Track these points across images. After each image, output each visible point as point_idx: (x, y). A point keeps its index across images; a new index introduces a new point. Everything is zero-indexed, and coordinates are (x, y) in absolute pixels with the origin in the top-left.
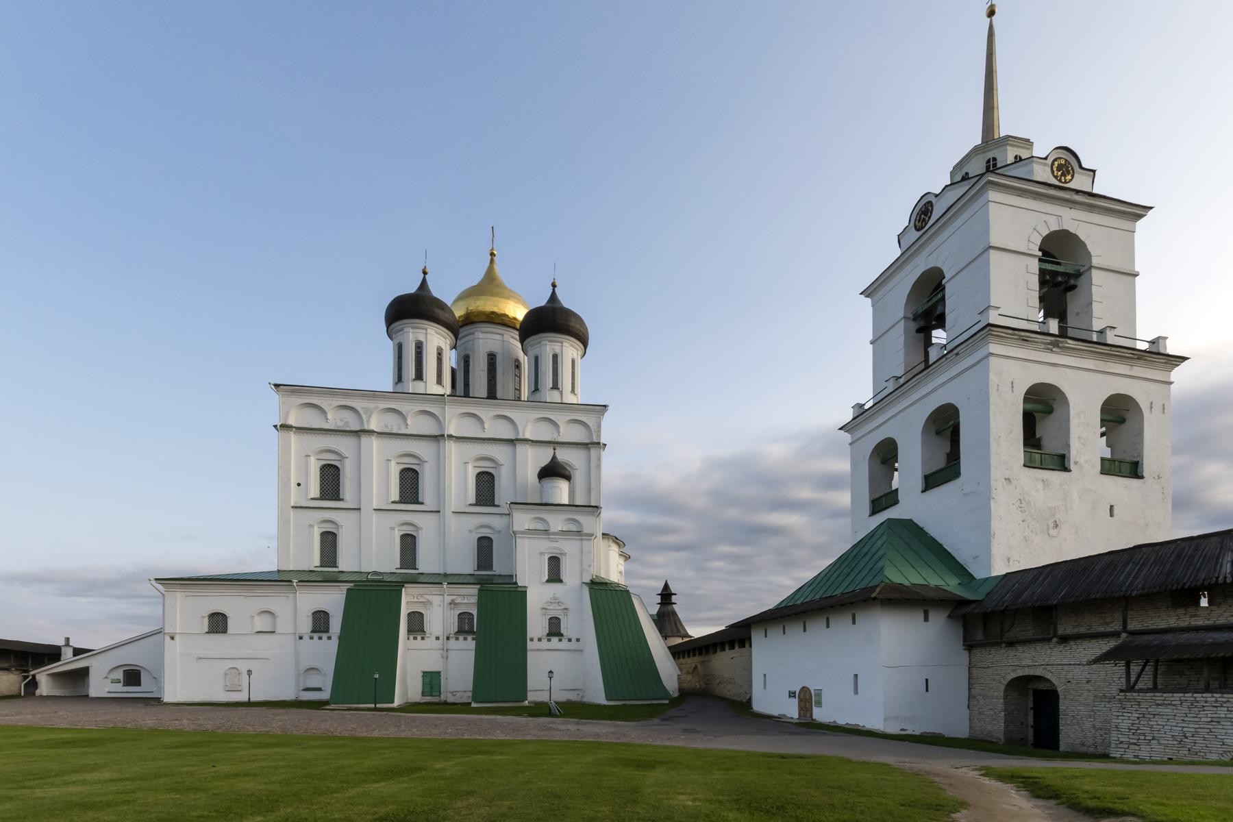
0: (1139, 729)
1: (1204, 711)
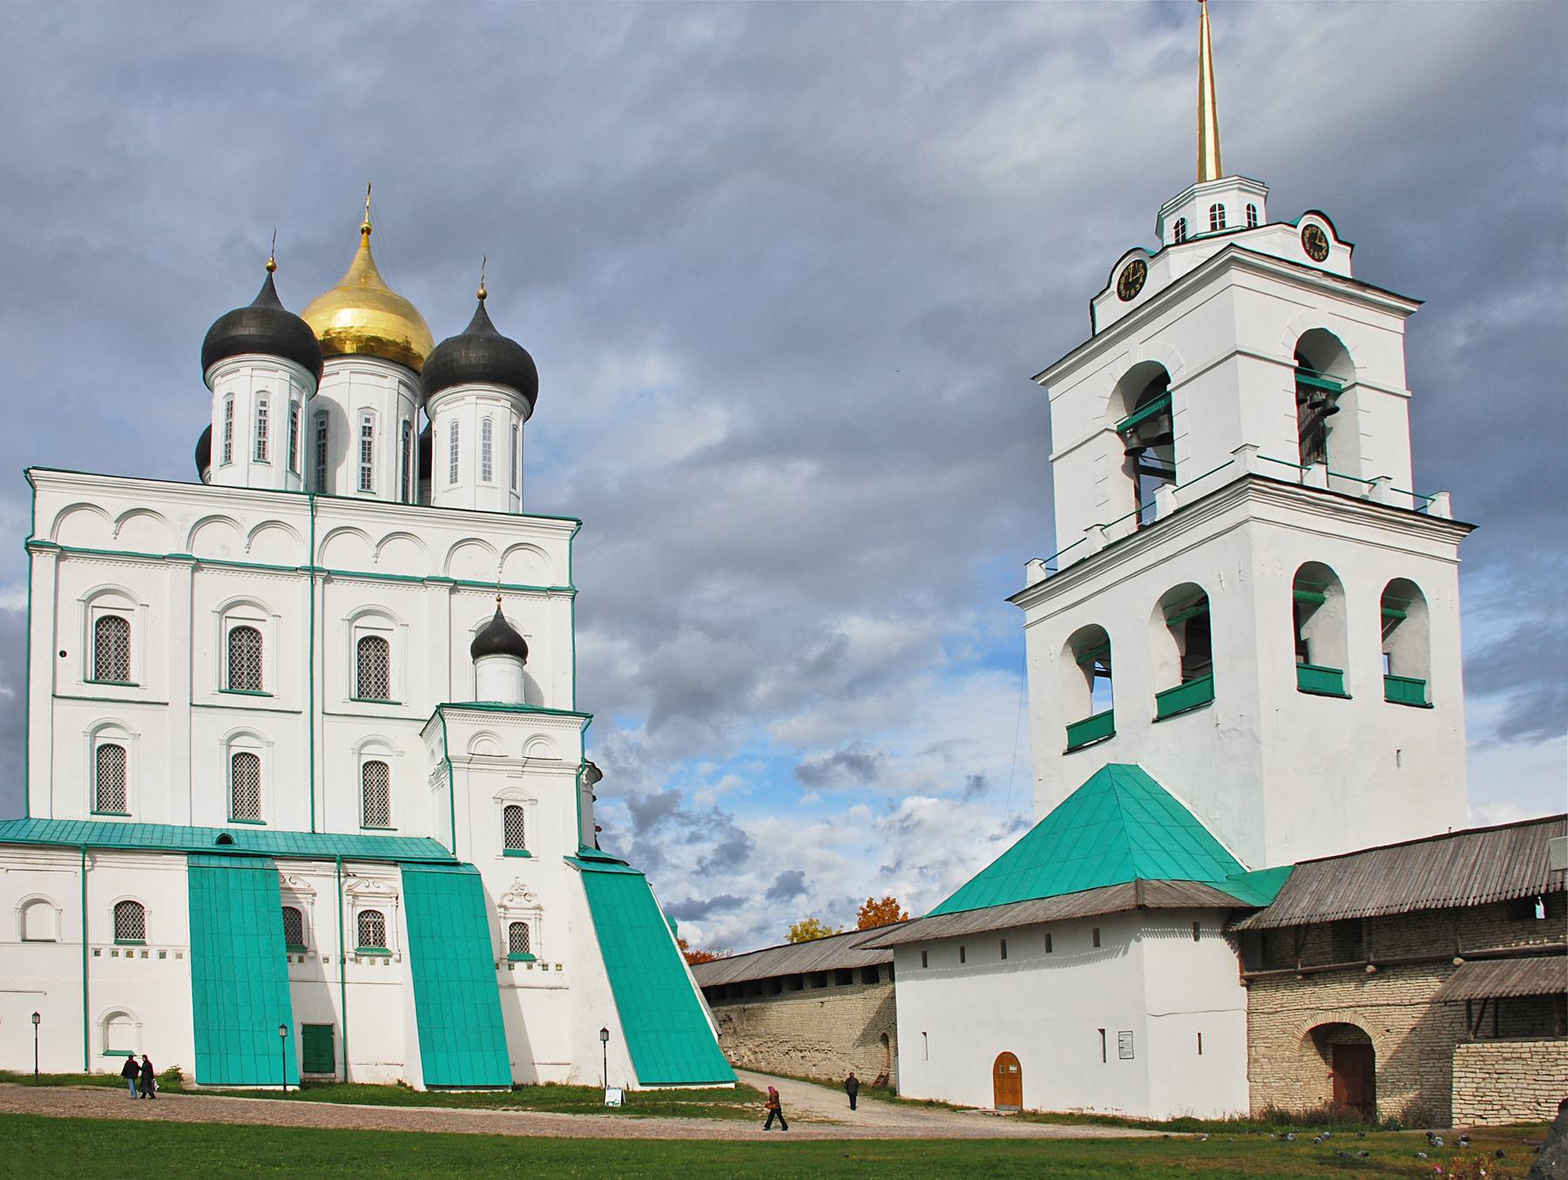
0: (1484, 1095)
1: (1557, 1065)
